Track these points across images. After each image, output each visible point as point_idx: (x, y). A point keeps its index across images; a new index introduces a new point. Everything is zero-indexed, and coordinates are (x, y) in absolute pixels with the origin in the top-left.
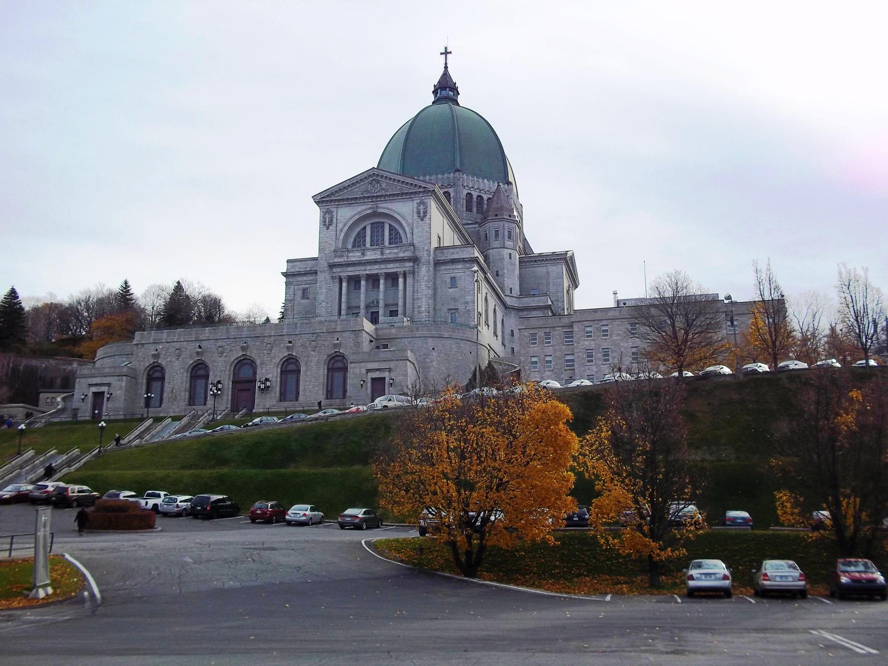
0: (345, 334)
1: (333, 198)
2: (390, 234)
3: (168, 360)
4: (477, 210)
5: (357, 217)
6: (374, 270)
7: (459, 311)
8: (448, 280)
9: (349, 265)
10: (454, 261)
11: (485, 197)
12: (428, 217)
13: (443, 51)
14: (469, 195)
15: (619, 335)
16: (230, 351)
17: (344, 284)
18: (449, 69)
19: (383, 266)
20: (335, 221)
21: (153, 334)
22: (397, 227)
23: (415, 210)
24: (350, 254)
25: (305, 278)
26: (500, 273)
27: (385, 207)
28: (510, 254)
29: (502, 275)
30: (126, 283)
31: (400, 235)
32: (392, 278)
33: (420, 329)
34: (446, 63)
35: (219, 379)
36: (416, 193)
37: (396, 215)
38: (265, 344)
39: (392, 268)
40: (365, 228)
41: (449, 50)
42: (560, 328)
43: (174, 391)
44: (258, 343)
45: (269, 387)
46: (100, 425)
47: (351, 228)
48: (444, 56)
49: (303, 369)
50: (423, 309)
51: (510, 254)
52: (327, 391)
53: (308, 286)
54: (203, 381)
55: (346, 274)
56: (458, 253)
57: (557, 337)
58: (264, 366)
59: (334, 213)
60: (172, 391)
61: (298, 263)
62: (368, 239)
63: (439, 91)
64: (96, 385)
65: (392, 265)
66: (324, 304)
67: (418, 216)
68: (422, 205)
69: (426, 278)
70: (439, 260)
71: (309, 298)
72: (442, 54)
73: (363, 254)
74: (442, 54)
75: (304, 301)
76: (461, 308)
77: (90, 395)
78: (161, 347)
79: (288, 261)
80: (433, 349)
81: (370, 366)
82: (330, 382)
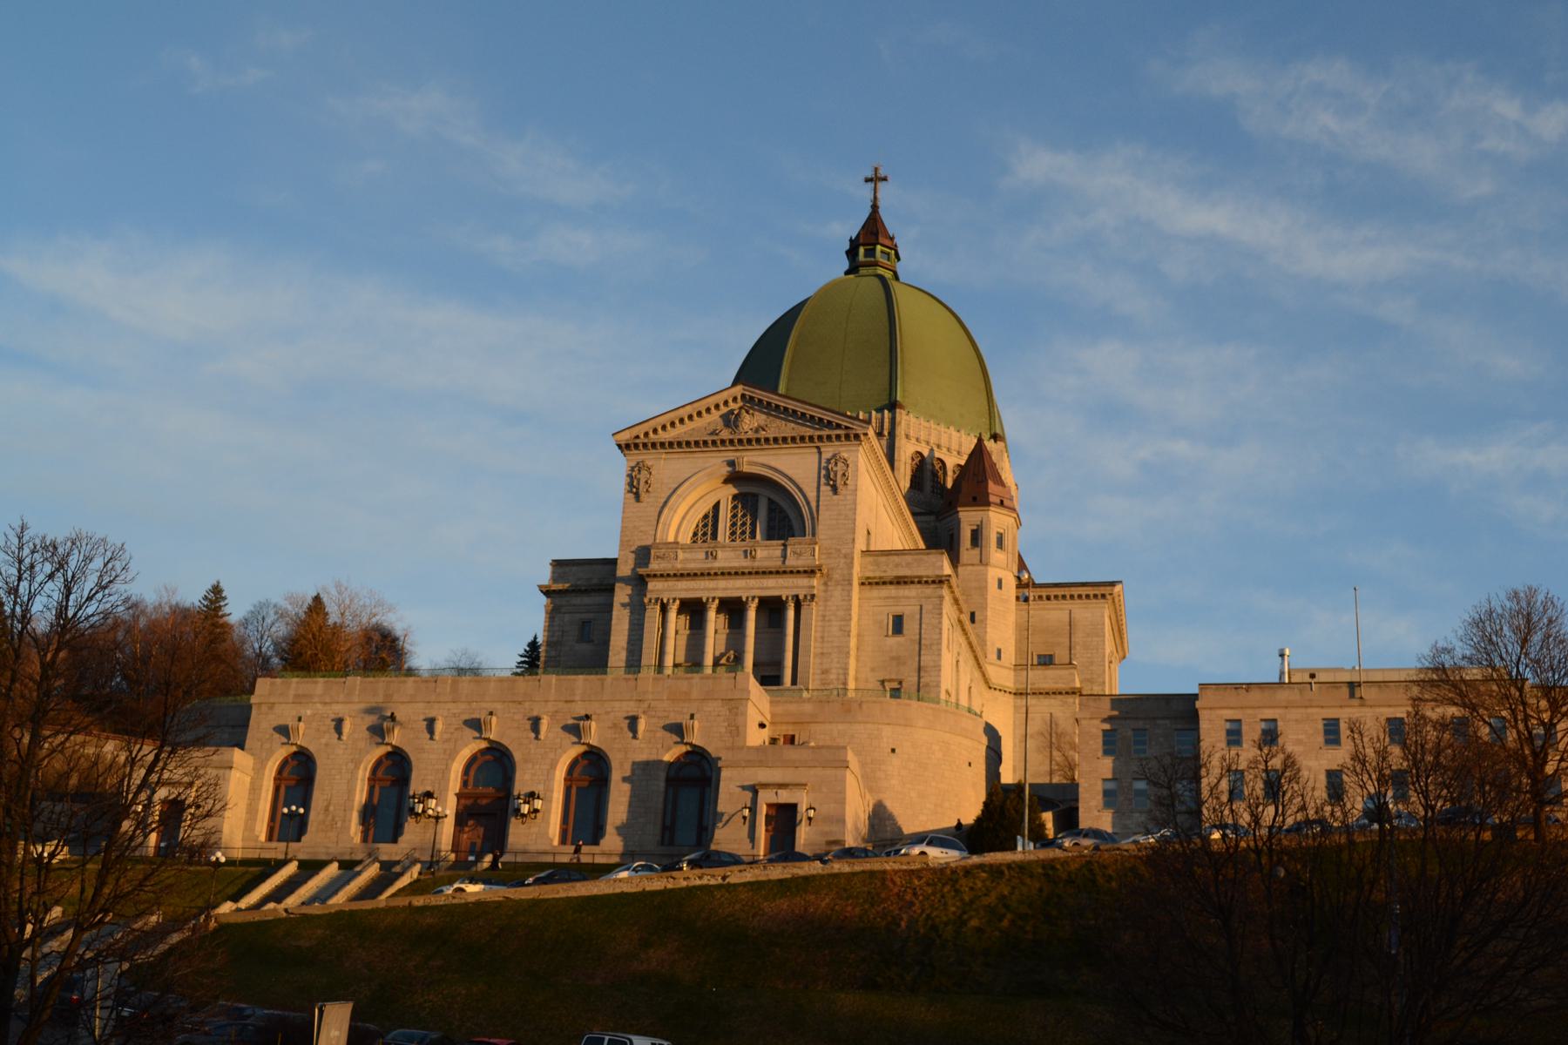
0: (713, 707)
3: (323, 741)
4: (933, 487)
7: (904, 684)
10: (900, 581)
12: (849, 487)
13: (870, 174)
15: (1299, 742)
16: (456, 729)
17: (672, 615)
18: (880, 210)
19: (753, 582)
21: (294, 685)
22: (784, 504)
23: (823, 472)
24: (688, 555)
25: (587, 600)
26: (977, 618)
28: (1000, 581)
29: (982, 621)
30: (217, 590)
31: (790, 521)
32: (772, 609)
33: (864, 706)
34: (875, 198)
35: (429, 788)
36: (829, 438)
41: (882, 173)
42: (1167, 722)
43: (331, 808)
44: (516, 717)
45: (536, 811)
46: (213, 858)
48: (871, 185)
50: (833, 677)
51: (1000, 581)
52: (664, 828)
53: (591, 616)
56: (908, 565)
57: (1161, 739)
58: (530, 766)
60: (327, 809)
61: (574, 568)
63: (862, 250)
67: (828, 484)
68: (840, 464)
69: (841, 613)
70: (868, 578)
71: (593, 641)
72: (867, 180)
74: (867, 180)
78: (309, 712)
79: (558, 564)
80: (893, 751)
81: (762, 775)
82: (670, 807)
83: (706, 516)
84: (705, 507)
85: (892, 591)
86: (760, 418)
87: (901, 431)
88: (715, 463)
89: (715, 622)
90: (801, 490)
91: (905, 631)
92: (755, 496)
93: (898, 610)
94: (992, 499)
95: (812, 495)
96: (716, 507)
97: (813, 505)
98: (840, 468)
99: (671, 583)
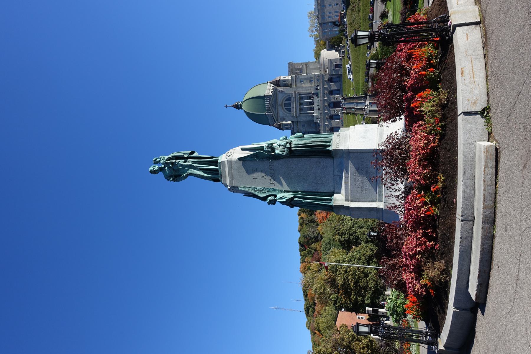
2: (287, 101)
5: (283, 111)
6: (298, 104)
9: (296, 111)
11: (272, 88)
14: (271, 92)
17: (302, 112)
22: (285, 99)
25: (299, 126)
37: (282, 99)
39: (298, 98)
40: (285, 109)
47: (286, 112)
54: (334, 117)
55: (299, 112)
62: (288, 107)
65: (297, 99)
71: (305, 125)
75: (306, 125)
83: (287, 110)
85: (297, 83)
87: (268, 95)
92: (284, 103)
94: (279, 79)
99: (297, 113)
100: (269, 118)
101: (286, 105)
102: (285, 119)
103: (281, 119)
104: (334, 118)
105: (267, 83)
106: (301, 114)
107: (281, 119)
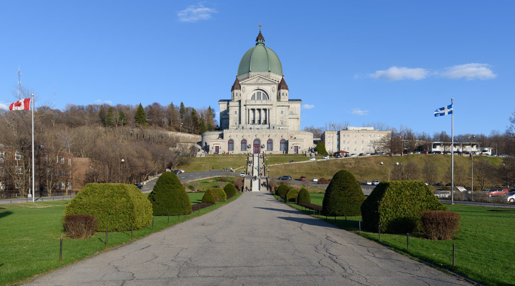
0: (285, 134)
1: (245, 83)
8: (281, 112)
10: (282, 106)
13: (259, 25)
19: (262, 106)
20: (246, 91)
23: (272, 89)
25: (235, 108)
27: (261, 87)
32: (265, 110)
38: (262, 135)
39: (265, 107)
49: (274, 142)
54: (244, 144)
56: (283, 104)
59: (246, 88)
60: (236, 147)
63: (259, 40)
64: (216, 144)
66: (243, 117)
73: (256, 102)
76: (285, 120)
77: (215, 147)
81: (294, 143)
83: (253, 95)
84: (253, 94)
85: (281, 107)
86: (261, 80)
87: (270, 76)
88: (256, 87)
89: (257, 111)
90: (268, 92)
91: (283, 113)
93: (282, 110)
95: (270, 93)
96: (255, 94)
97: (270, 94)
98: (274, 89)
100: (245, 76)
101: (259, 94)
102: (244, 93)
103: (244, 87)
104: (243, 144)
105: (283, 76)
106: (248, 110)
107: (244, 87)
